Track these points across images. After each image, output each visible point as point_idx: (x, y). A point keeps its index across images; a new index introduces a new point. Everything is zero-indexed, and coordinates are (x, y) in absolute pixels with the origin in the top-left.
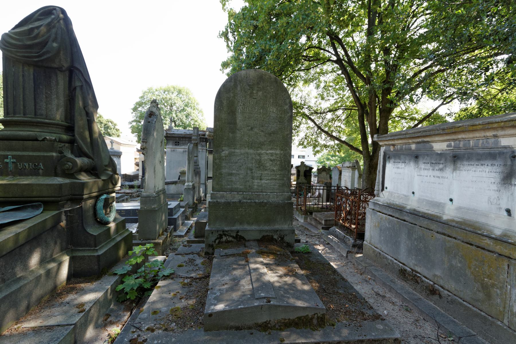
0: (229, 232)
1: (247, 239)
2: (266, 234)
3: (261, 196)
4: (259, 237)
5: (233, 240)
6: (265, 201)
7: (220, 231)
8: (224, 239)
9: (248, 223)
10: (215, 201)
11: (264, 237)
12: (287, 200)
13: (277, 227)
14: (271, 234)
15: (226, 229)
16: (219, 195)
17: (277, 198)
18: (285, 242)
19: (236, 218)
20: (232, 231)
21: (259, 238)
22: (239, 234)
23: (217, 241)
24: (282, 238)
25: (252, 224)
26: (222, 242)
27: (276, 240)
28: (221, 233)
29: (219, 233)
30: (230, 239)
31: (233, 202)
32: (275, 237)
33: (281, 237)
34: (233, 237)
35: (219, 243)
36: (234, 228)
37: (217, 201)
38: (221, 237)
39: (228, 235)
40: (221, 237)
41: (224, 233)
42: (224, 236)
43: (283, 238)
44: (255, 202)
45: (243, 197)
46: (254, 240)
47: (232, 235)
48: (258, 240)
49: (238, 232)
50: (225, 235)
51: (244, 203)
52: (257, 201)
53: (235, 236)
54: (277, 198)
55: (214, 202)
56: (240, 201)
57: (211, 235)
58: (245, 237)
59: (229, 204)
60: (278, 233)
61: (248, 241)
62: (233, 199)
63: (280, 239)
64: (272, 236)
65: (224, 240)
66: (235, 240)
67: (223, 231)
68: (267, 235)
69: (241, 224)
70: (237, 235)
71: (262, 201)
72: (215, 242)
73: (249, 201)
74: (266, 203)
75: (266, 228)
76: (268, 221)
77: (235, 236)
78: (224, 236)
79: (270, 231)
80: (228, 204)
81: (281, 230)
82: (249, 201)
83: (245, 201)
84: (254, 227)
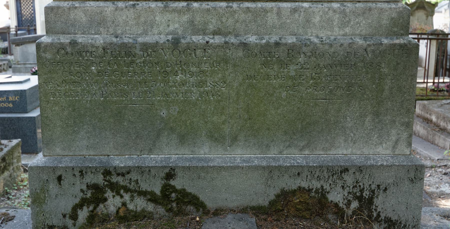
0: (134, 176)
1: (210, 205)
2: (292, 184)
3: (272, 19)
4: (263, 195)
5: (150, 207)
6: (291, 40)
7: (95, 170)
8: (113, 203)
9: (217, 138)
10: (65, 39)
11: (285, 195)
12: (390, 34)
13: (344, 151)
14: (316, 184)
15: (119, 162)
16: (79, 16)
17: (343, 25)
18: (378, 219)
19: (164, 113)
20: (141, 170)
21: (264, 201)
22: (177, 183)
23: (83, 214)
24: (367, 203)
25: (235, 139)
26: (105, 219)
27: (339, 213)
28: (99, 179)
29: (90, 179)
30: (140, 204)
31: (145, 47)
32: (336, 196)
33: (360, 199)
34: (152, 198)
35: (92, 218)
36: (154, 159)
37: (73, 43)
38: (96, 196)
39: (127, 190)
40: (96, 196)
41: (110, 181)
42: (109, 194)
43: (370, 201)
44: (244, 45)
45: (192, 22)
46: (244, 210)
47: (144, 187)
48: (257, 211)
49: (170, 175)
50: (116, 189)
51: (192, 48)
52: (252, 39)
53: (158, 191)
54: (343, 25)
55: (62, 47)
56: (176, 42)
57: (53, 187)
58: (202, 198)
59: (129, 54)
60: (349, 179)
61: (218, 212)
62: (145, 33)
63: (355, 205)
64: (323, 193)
65: (112, 209)
66: (161, 210)
67: (107, 173)
68: (300, 189)
69: (183, 139)
70: (167, 189)
71: (274, 39)
72: (74, 217)
73: (218, 40)
74: (293, 51)
75: (296, 157)
76: (303, 129)
77: (158, 191)
78: (109, 194)
79: (311, 170)
80: (121, 55)
81: (360, 169)
82: (218, 40)
83: (198, 39)
84: (240, 155)
